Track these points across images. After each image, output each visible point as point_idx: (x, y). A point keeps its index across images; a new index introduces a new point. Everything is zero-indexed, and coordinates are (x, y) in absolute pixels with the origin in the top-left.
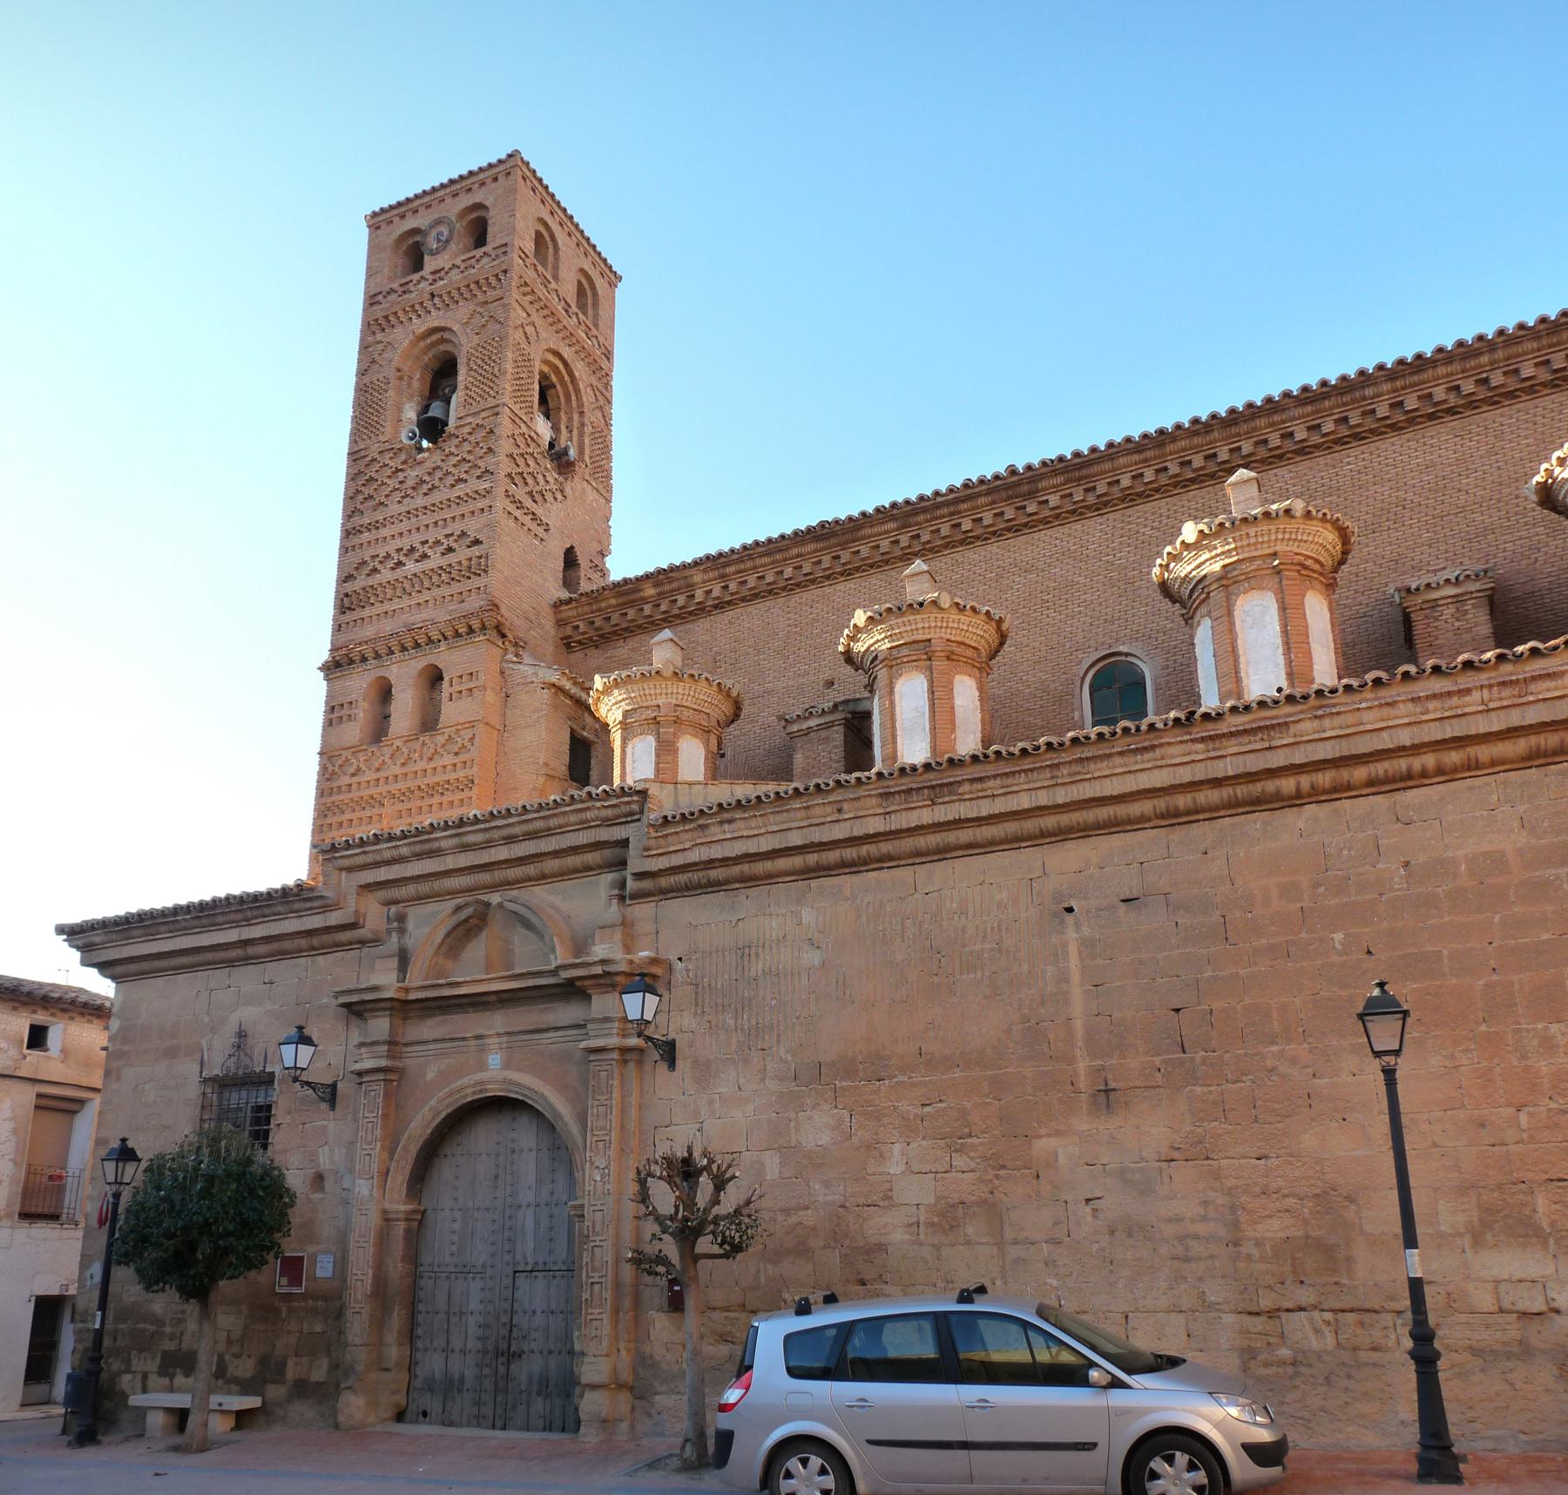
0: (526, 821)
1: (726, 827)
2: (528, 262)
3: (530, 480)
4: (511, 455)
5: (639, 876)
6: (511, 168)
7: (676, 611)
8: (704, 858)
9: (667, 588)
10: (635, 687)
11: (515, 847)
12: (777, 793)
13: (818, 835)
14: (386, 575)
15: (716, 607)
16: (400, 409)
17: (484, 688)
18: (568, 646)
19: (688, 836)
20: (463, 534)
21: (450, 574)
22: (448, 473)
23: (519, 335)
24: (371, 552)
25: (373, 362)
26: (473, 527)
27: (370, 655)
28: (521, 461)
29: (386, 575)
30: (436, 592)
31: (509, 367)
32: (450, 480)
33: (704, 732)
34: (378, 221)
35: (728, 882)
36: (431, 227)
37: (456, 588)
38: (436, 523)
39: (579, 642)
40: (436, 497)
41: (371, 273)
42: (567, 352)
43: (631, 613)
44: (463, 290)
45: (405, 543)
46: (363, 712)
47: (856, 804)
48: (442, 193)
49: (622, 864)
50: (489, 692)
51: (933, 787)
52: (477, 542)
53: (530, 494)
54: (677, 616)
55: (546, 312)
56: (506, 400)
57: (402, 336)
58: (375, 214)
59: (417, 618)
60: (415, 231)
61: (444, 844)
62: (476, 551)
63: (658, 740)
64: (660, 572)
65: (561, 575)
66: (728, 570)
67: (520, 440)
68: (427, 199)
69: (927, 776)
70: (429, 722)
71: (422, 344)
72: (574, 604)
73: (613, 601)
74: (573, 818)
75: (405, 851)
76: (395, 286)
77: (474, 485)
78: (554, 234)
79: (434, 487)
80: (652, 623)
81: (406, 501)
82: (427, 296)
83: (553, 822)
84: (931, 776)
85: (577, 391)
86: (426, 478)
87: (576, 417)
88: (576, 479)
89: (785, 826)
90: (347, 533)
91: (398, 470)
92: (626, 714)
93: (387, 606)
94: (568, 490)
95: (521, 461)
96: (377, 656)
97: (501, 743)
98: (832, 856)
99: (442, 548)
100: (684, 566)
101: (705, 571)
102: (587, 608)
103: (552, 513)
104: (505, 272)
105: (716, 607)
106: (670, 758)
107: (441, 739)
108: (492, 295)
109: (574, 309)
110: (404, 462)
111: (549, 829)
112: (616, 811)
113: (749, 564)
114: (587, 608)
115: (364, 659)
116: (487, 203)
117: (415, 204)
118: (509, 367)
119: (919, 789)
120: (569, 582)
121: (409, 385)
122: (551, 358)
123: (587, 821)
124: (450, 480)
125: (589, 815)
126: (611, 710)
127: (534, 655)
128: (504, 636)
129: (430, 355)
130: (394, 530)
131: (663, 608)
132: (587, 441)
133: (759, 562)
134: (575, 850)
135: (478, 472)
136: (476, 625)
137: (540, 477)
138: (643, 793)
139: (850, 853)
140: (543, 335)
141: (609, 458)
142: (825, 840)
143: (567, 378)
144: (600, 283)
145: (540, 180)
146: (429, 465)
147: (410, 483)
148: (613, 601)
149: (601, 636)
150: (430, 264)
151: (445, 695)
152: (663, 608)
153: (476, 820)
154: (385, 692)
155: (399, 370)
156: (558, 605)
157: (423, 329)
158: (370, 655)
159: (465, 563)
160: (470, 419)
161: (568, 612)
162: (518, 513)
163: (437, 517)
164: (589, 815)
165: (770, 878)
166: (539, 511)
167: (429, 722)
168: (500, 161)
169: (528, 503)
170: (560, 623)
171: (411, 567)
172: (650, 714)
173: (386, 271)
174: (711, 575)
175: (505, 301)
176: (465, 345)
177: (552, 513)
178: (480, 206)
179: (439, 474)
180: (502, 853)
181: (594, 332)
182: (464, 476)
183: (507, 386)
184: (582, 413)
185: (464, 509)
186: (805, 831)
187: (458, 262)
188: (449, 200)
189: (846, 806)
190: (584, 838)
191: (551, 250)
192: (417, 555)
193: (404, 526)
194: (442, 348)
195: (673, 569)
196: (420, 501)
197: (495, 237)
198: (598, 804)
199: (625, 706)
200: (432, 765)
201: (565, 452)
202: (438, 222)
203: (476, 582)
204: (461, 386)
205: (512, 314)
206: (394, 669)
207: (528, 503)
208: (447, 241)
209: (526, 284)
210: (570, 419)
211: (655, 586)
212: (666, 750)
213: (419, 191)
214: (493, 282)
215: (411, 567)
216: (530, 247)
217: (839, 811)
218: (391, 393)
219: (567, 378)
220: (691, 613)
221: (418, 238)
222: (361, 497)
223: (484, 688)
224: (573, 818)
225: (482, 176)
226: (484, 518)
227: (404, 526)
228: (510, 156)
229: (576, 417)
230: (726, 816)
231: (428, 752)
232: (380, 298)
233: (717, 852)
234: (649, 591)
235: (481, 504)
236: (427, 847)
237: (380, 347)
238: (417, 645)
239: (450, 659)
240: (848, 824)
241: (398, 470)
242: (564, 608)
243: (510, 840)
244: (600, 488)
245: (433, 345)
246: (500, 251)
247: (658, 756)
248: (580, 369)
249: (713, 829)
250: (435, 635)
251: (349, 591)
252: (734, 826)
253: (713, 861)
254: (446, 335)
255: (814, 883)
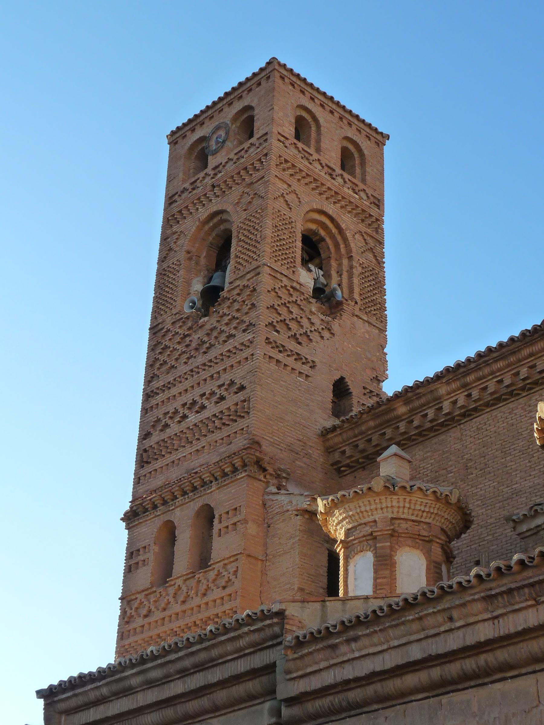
0: (193, 653)
1: (353, 645)
2: (287, 143)
3: (293, 325)
4: (272, 307)
5: (291, 701)
6: (273, 72)
7: (428, 425)
8: (339, 679)
9: (417, 404)
10: (352, 505)
11: (188, 680)
12: (390, 606)
13: (437, 647)
14: (175, 428)
15: (464, 415)
16: (189, 283)
17: (246, 521)
18: (339, 471)
19: (321, 656)
20: (232, 383)
21: (223, 420)
22: (222, 331)
23: (280, 204)
24: (163, 410)
25: (170, 249)
26: (238, 375)
27: (158, 502)
28: (283, 311)
29: (175, 428)
30: (211, 437)
31: (268, 232)
32: (223, 337)
33: (422, 542)
34: (175, 137)
35: (366, 703)
36: (213, 133)
37: (226, 431)
38: (212, 376)
39: (348, 466)
40: (212, 354)
41: (170, 179)
42: (331, 209)
43: (389, 432)
44: (236, 177)
45: (187, 398)
46: (152, 556)
47: (464, 611)
48: (220, 105)
49: (271, 692)
50: (250, 524)
51: (532, 585)
52: (242, 388)
53: (294, 336)
54: (431, 429)
55: (307, 180)
56: (266, 260)
57: (190, 226)
58: (173, 133)
59: (195, 463)
60: (203, 139)
61: (135, 681)
62: (241, 396)
63: (376, 556)
64: (407, 390)
65: (330, 406)
66: (470, 378)
67: (282, 293)
68: (210, 112)
69: (525, 574)
70: (203, 561)
71: (206, 228)
72: (338, 431)
73: (372, 424)
74: (229, 647)
75: (105, 691)
76: (187, 185)
77: (243, 338)
78: (313, 114)
79: (211, 346)
80: (409, 439)
81: (191, 361)
82: (209, 188)
83: (215, 653)
84: (529, 573)
85: (345, 240)
86: (206, 339)
87: (345, 262)
88: (345, 316)
89: (403, 640)
90: (148, 396)
91: (185, 336)
92: (348, 533)
93: (174, 457)
94: (335, 326)
95: (283, 311)
96: (165, 503)
97: (264, 573)
98: (454, 669)
99: (214, 399)
100: (428, 382)
101: (448, 383)
102: (350, 433)
103: (318, 350)
104: (266, 155)
105: (464, 415)
106: (387, 572)
107: (212, 575)
108: (257, 175)
109: (339, 171)
110: (190, 329)
111: (212, 660)
112: (262, 635)
113: (486, 371)
114: (350, 433)
115: (155, 507)
116: (253, 105)
117: (201, 118)
118: (268, 232)
119: (519, 589)
120: (337, 412)
121: (197, 263)
122: (316, 216)
123: (241, 649)
124: (223, 337)
125: (242, 643)
126: (337, 528)
127: (300, 483)
128: (265, 470)
129: (214, 234)
130: (180, 388)
131: (416, 423)
132: (356, 281)
133: (495, 367)
134: (236, 679)
135: (244, 326)
136: (238, 463)
137: (305, 322)
138: (281, 614)
139: (469, 664)
140: (305, 198)
141: (383, 292)
142: (441, 651)
143: (334, 230)
144: (365, 145)
145: (298, 76)
146: (208, 327)
147: (194, 345)
148: (372, 424)
149: (367, 457)
150: (212, 161)
151: (215, 531)
152: (416, 423)
153: (154, 657)
154: (170, 533)
155: (188, 252)
156: (325, 433)
157: (206, 215)
158: (158, 502)
159: (233, 408)
160: (238, 283)
161: (335, 439)
162: (280, 357)
163: (212, 371)
164: (242, 643)
165: (402, 697)
166: (304, 351)
167: (203, 561)
168: (262, 70)
169: (292, 345)
170: (329, 450)
171: (193, 418)
172: (368, 530)
173: (181, 175)
174: (454, 386)
175: (266, 179)
176: (237, 219)
177: (318, 350)
178: (249, 108)
179: (215, 334)
180: (178, 687)
181: (361, 186)
182: (233, 332)
183: (267, 248)
184: (350, 258)
185: (233, 361)
186: (424, 643)
187: (231, 156)
188: (226, 109)
189: (455, 614)
190: (242, 666)
191: (314, 128)
192: (197, 408)
193: (187, 384)
194: (222, 227)
195: (418, 385)
196: (200, 359)
197: (259, 128)
198: (246, 629)
199: (347, 525)
200: (205, 600)
201: (333, 294)
202: (218, 128)
203: (242, 424)
204: (232, 256)
205: (271, 188)
206: (178, 512)
207: (292, 345)
208: (224, 142)
209: (286, 161)
210: (340, 265)
211: (407, 402)
212: (385, 565)
213: (203, 108)
214: (257, 165)
215: (193, 418)
216: (289, 130)
217: (451, 619)
218: (182, 272)
219: (334, 230)
220: (442, 425)
221: (204, 145)
222: (157, 365)
223: (246, 521)
224: (229, 647)
225: (249, 84)
226: (247, 367)
227: (187, 384)
228: (268, 63)
229: (345, 262)
230: (351, 633)
231: (202, 588)
232: (176, 197)
233: (348, 672)
234: (402, 410)
235: (246, 353)
236: (121, 685)
237: (175, 236)
238: (194, 489)
239: (220, 498)
240: (460, 633)
241: (185, 336)
242: (330, 436)
243: (184, 673)
244: (373, 320)
245: (215, 226)
246: (261, 141)
247: (376, 572)
248: (347, 221)
249: (344, 648)
250: (207, 477)
251: (146, 446)
252: (360, 643)
253: (347, 682)
254: (224, 216)
255: (444, 699)
